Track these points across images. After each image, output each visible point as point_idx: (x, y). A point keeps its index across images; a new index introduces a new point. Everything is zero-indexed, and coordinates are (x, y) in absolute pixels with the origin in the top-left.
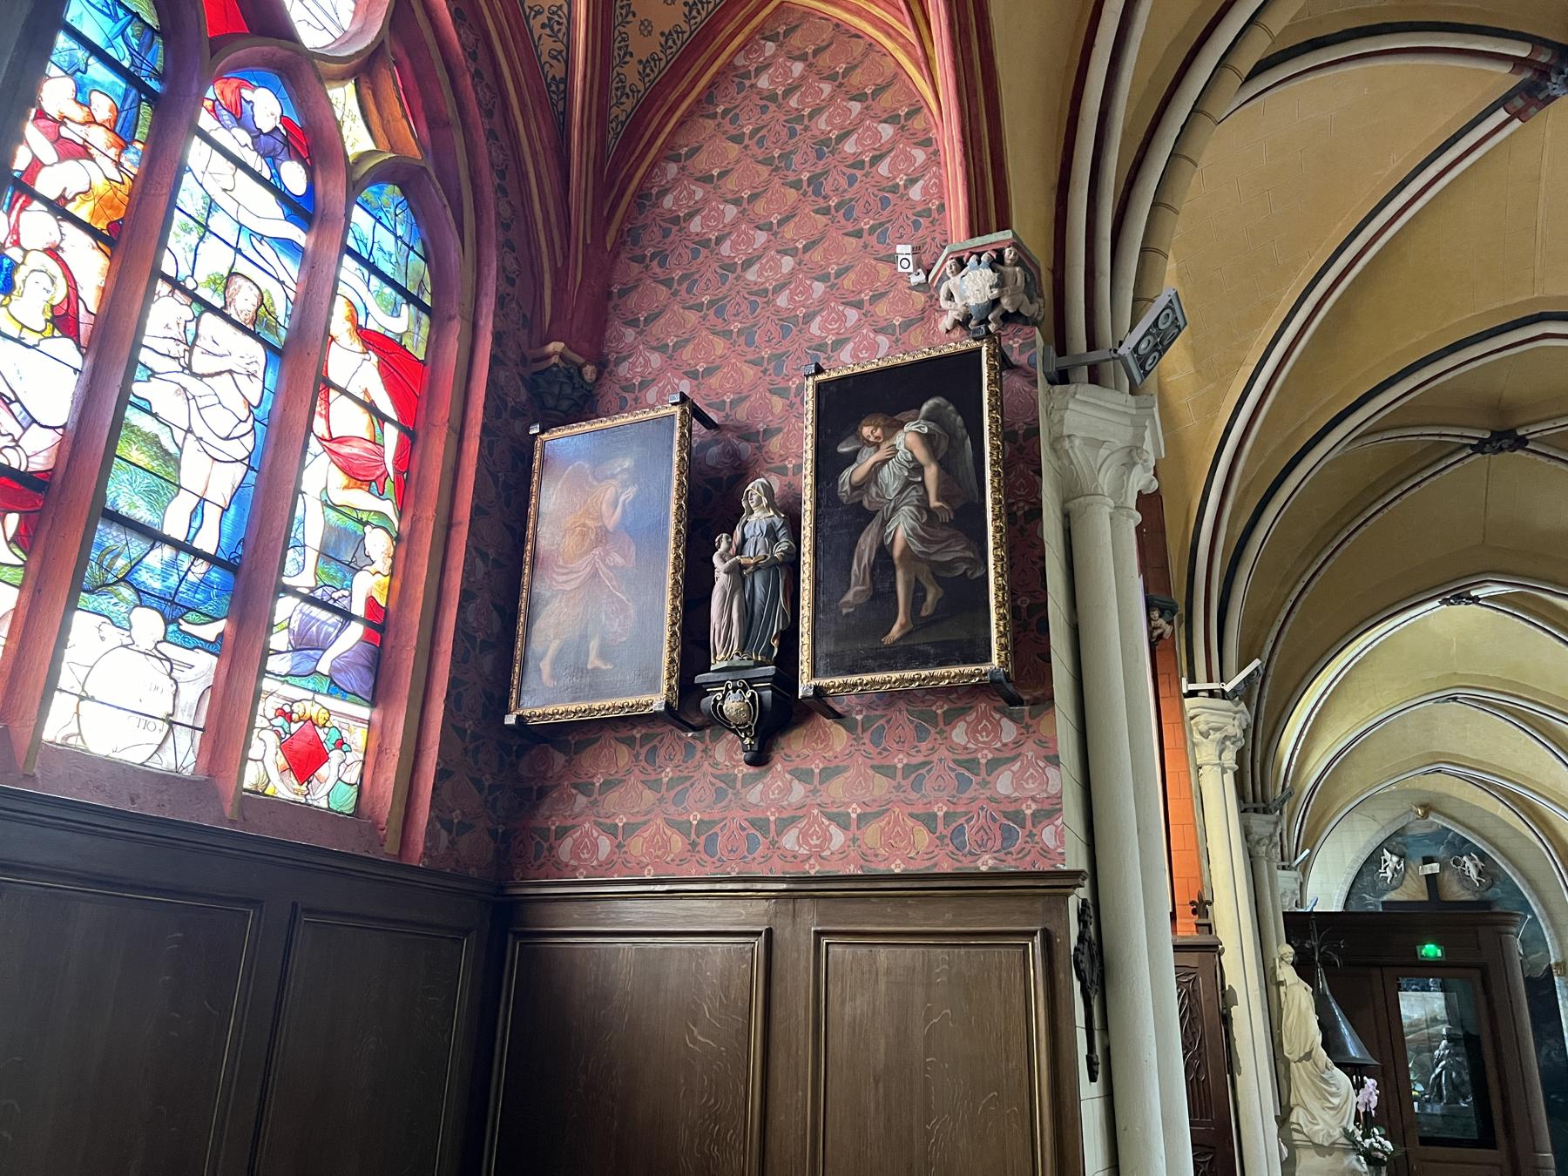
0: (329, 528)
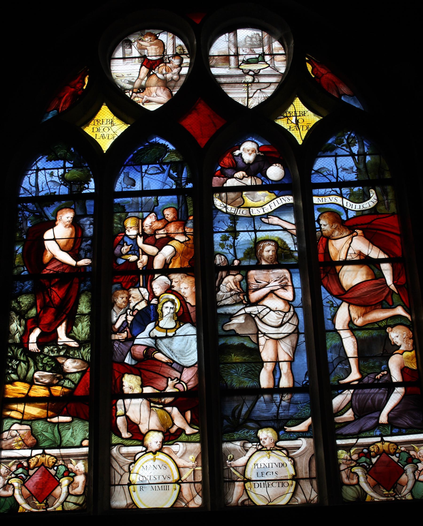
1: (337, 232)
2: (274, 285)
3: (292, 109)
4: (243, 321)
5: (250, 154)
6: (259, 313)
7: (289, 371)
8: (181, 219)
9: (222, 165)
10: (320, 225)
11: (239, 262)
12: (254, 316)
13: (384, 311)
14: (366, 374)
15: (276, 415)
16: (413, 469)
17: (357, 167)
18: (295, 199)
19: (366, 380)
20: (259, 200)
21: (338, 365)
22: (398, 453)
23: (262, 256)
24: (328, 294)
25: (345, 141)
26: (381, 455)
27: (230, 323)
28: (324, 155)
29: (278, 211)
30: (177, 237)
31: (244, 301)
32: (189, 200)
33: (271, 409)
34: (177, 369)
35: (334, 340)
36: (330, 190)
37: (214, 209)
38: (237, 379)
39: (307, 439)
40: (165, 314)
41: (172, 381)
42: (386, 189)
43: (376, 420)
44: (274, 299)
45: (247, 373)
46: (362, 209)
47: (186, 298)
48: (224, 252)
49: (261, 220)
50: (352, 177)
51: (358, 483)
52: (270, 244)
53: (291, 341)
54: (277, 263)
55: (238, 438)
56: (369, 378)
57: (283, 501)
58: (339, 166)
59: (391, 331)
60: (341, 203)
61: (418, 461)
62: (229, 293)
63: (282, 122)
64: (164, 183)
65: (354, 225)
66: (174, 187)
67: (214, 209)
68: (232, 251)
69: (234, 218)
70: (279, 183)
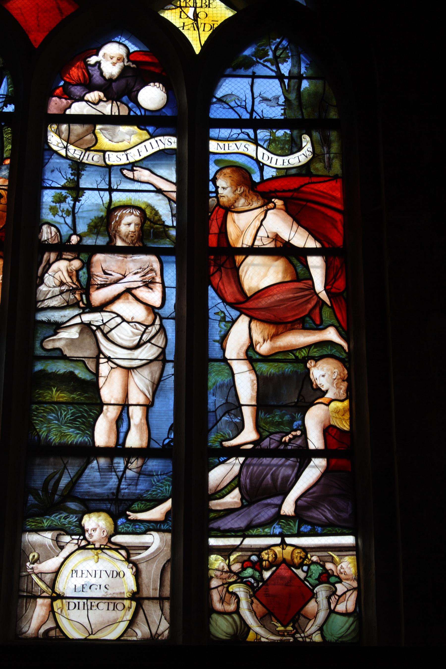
0: (262, 382)
1: (242, 201)
2: (133, 280)
4: (77, 336)
5: (114, 64)
6: (104, 324)
7: (144, 421)
10: (217, 188)
11: (79, 238)
12: (94, 328)
13: (306, 333)
14: (267, 433)
15: (115, 491)
16: (328, 593)
17: (285, 97)
18: (179, 143)
19: (265, 443)
20: (121, 140)
21: (224, 415)
22: (306, 565)
23: (118, 232)
24: (220, 301)
25: (270, 53)
26: (278, 566)
27: (55, 337)
28: (235, 73)
29: (151, 160)
31: (81, 303)
33: (108, 482)
35: (222, 375)
36: (239, 131)
38: (56, 429)
39: (162, 534)
42: (329, 136)
43: (277, 509)
44: (131, 302)
45: (75, 420)
46: (286, 165)
48: (55, 222)
49: (122, 173)
50: (276, 113)
51: (237, 611)
52: (133, 213)
53: (151, 372)
54: (141, 245)
55: (50, 526)
56: (272, 441)
57: (113, 634)
58: (256, 94)
59: (315, 366)
61: (337, 579)
62: (58, 289)
63: (171, 16)
65: (271, 192)
68: (69, 220)
69: (78, 167)
70: (157, 114)
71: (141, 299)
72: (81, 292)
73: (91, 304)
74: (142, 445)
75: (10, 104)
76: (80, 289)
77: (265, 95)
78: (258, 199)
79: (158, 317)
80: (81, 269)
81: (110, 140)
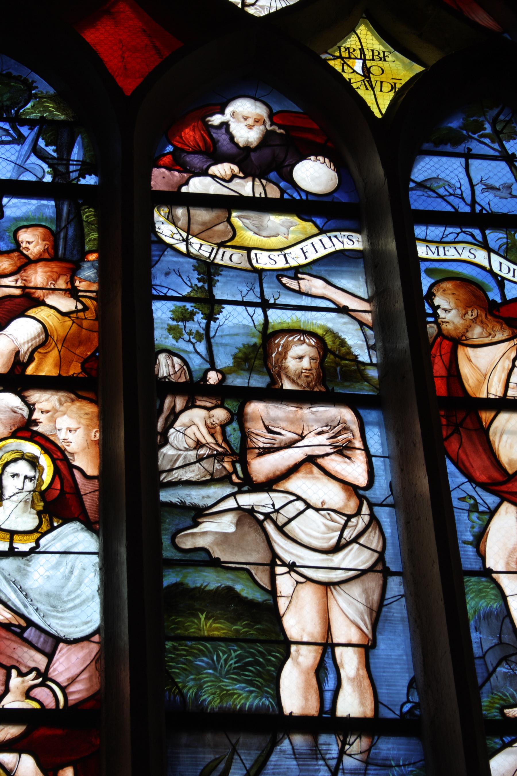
1: (477, 332)
3: (353, 43)
4: (232, 529)
5: (250, 127)
6: (277, 511)
7: (363, 672)
8: (64, 256)
9: (176, 143)
10: (435, 308)
11: (220, 376)
12: (261, 517)
20: (273, 233)
21: (499, 664)
23: (282, 369)
29: (324, 265)
30: (51, 300)
31: (234, 477)
32: (88, 215)
34: (39, 645)
35: (484, 597)
37: (154, 242)
38: (213, 684)
40: (7, 493)
41: (20, 679)
44: (318, 478)
45: (244, 668)
47: (72, 454)
48: (179, 349)
52: (304, 341)
53: (365, 591)
60: (486, 264)
62: (193, 453)
64: (22, 168)
66: (48, 179)
67: (154, 242)
68: (202, 347)
69: (209, 270)
71: (333, 473)
72: (234, 458)
73: (252, 478)
74: (365, 712)
75: (90, 175)
76: (230, 455)
77: (490, 182)
78: (502, 329)
79: (365, 502)
80: (229, 422)
81: (256, 233)
